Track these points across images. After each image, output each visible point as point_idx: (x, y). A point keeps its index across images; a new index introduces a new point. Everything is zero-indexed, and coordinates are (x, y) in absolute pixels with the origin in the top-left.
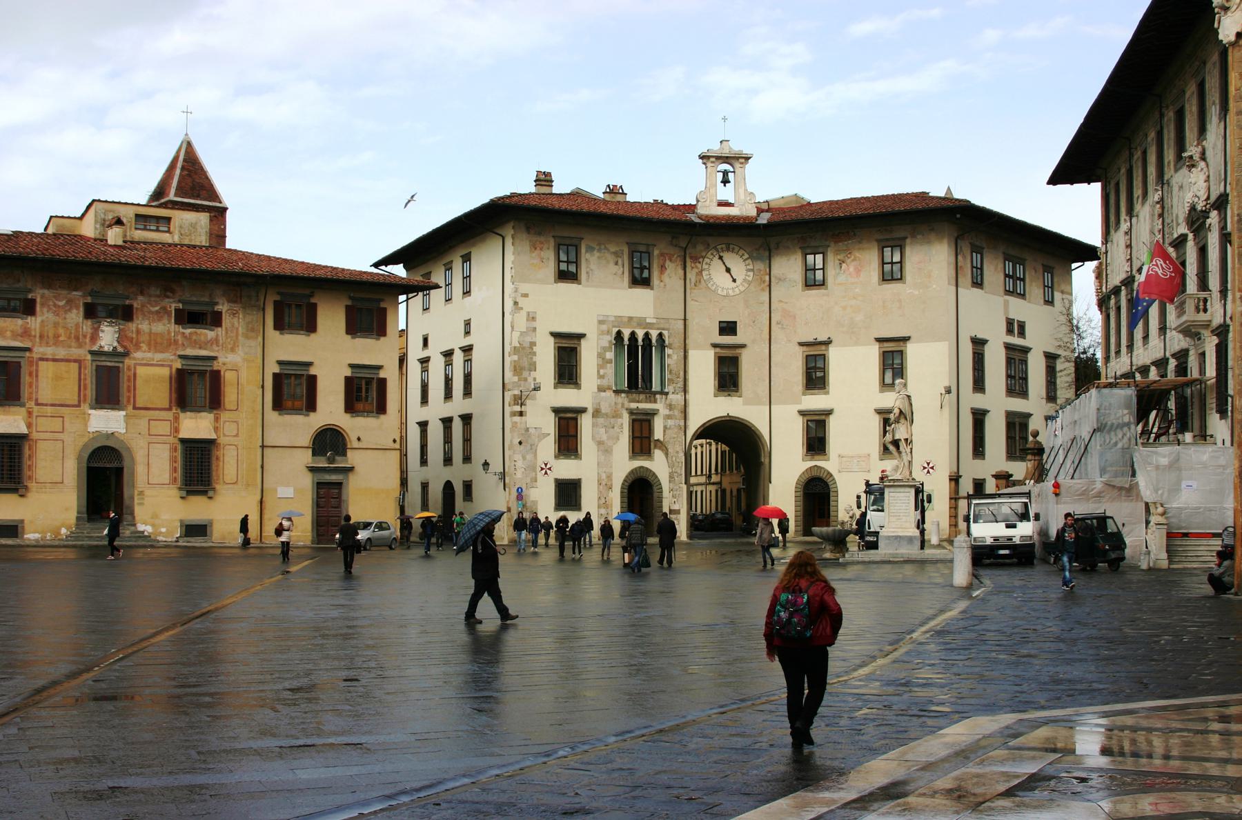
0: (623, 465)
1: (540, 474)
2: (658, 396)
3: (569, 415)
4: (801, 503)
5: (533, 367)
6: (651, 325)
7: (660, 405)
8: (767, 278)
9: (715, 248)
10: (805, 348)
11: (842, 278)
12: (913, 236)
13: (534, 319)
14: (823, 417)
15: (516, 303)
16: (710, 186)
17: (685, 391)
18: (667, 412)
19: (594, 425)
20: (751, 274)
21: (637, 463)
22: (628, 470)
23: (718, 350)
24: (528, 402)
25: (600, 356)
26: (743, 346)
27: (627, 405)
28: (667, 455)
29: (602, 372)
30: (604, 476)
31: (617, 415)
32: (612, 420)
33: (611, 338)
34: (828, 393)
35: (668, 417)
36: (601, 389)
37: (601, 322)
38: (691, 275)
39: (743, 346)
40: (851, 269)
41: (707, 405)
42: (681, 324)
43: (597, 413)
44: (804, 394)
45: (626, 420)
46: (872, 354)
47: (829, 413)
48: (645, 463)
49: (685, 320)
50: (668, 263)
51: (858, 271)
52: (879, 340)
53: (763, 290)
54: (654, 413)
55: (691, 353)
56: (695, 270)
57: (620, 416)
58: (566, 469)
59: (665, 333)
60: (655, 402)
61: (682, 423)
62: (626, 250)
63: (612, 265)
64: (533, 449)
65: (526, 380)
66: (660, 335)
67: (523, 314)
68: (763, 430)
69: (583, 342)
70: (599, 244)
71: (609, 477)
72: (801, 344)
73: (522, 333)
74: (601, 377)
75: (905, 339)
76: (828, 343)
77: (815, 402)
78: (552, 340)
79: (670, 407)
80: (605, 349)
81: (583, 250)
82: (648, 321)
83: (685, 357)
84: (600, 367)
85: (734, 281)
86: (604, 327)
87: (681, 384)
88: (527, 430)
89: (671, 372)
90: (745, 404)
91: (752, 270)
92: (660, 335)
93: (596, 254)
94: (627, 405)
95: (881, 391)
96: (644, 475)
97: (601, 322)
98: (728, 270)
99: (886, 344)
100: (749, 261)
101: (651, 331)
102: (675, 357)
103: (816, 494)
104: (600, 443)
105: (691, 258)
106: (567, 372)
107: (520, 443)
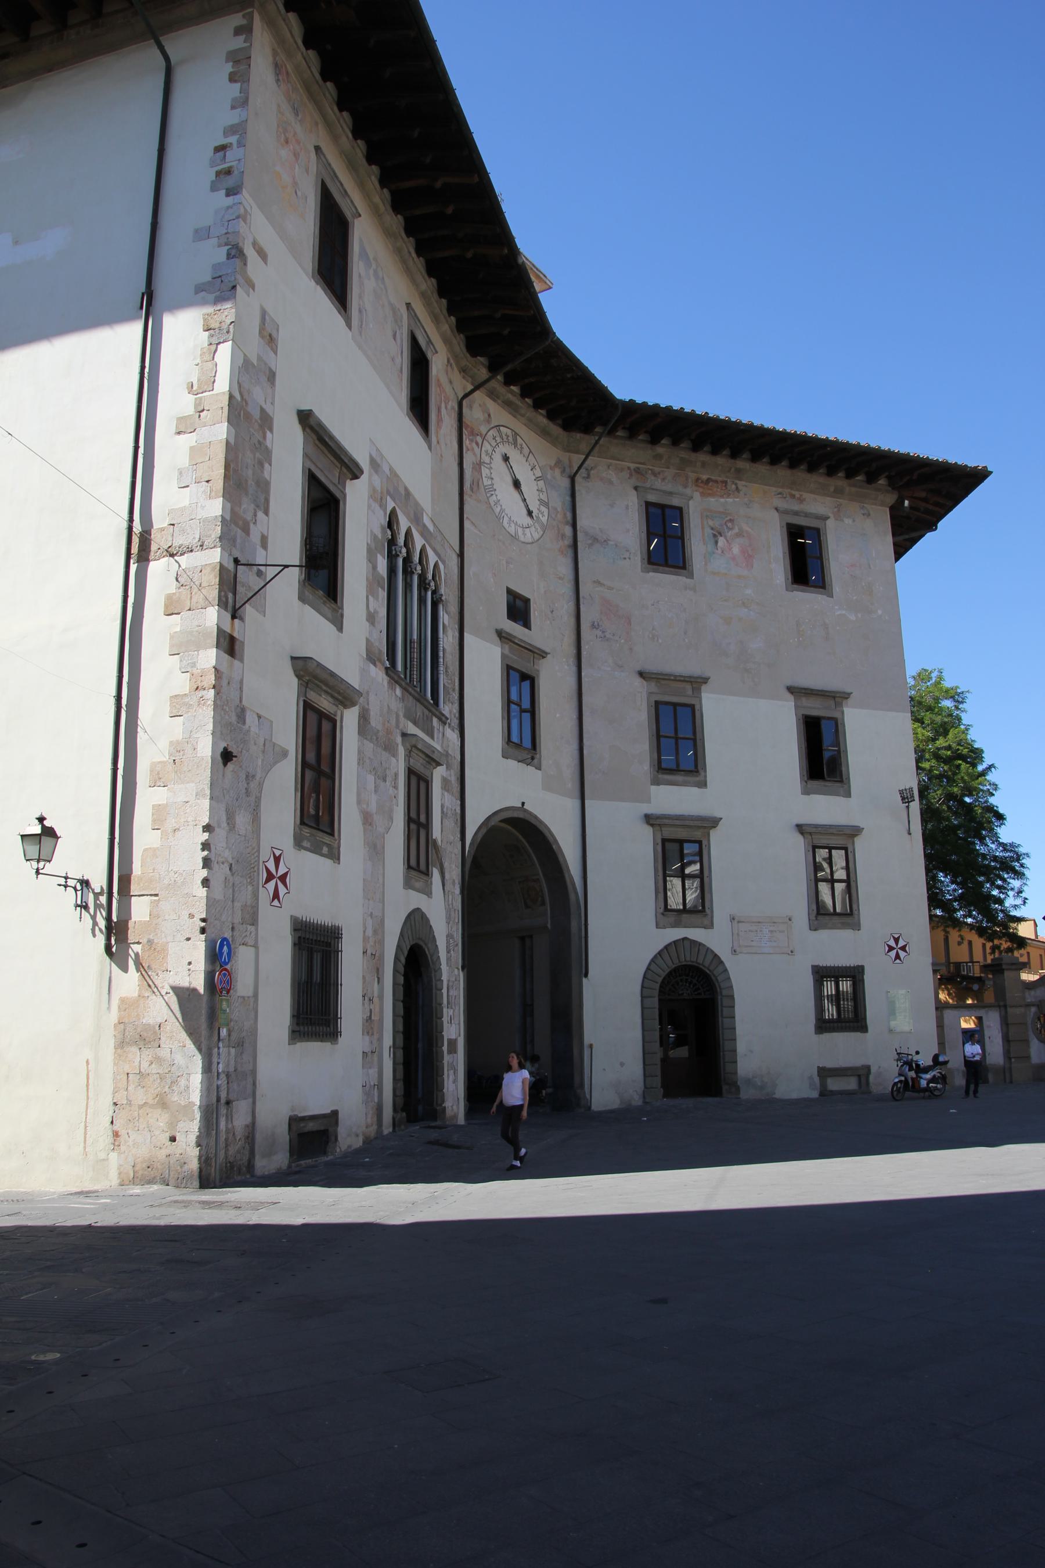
0: (400, 901)
3: (325, 703)
8: (568, 531)
10: (653, 687)
12: (838, 518)
13: (271, 340)
14: (697, 835)
15: (236, 253)
21: (416, 900)
26: (543, 654)
33: (381, 519)
34: (703, 784)
39: (543, 654)
44: (656, 782)
45: (399, 766)
47: (713, 822)
51: (748, 557)
61: (458, 811)
65: (246, 530)
71: (379, 929)
75: (846, 696)
76: (697, 683)
77: (676, 799)
82: (426, 521)
88: (241, 714)
90: (547, 786)
91: (546, 504)
94: (402, 719)
98: (517, 484)
99: (805, 702)
100: (541, 483)
103: (689, 1003)
104: (367, 819)
106: (322, 567)
107: (227, 756)
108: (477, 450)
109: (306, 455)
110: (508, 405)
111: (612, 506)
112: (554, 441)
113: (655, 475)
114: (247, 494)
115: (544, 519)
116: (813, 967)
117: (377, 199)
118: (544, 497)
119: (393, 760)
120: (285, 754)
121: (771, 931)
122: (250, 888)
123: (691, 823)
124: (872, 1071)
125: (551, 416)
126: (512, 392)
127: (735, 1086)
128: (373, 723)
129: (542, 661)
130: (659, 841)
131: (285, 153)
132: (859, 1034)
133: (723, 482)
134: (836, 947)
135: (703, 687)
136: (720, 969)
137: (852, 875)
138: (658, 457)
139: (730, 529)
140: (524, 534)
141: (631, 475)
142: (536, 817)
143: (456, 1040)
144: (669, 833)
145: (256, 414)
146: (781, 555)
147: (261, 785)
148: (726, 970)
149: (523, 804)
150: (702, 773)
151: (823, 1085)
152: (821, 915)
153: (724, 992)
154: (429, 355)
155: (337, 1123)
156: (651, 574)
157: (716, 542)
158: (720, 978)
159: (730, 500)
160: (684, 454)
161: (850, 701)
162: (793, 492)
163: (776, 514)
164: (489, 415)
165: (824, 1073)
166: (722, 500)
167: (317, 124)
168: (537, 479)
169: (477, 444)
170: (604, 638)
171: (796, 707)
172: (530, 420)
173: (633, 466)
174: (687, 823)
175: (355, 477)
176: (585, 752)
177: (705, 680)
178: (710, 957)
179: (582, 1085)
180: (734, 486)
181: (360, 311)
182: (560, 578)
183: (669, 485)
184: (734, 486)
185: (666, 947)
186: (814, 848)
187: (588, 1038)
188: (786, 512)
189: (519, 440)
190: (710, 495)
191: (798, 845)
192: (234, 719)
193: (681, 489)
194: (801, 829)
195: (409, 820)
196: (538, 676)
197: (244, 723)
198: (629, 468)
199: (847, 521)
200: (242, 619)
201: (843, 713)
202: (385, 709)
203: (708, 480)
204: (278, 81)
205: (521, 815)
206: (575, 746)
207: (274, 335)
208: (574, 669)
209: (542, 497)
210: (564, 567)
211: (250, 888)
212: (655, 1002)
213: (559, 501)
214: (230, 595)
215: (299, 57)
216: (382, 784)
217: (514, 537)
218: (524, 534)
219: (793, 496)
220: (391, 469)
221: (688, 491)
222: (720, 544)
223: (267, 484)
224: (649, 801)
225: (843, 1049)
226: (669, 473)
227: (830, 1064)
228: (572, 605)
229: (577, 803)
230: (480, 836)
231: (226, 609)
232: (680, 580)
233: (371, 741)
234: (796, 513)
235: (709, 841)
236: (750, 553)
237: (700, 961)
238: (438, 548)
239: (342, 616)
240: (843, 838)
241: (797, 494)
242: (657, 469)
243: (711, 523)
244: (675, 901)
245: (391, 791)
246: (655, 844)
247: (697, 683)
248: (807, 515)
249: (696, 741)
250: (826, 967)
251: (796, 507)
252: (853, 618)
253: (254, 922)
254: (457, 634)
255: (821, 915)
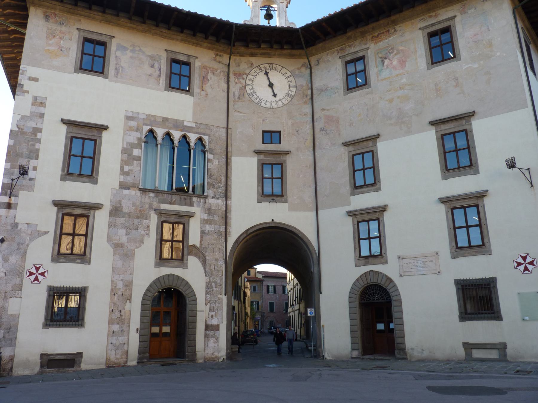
0: (146, 272)
1: (27, 282)
2: (195, 199)
4: (357, 316)
5: (35, 154)
6: (190, 129)
7: (197, 210)
8: (309, 92)
9: (259, 67)
10: (351, 148)
11: (385, 73)
12: (463, 12)
13: (42, 104)
14: (376, 216)
16: (255, 15)
17: (227, 196)
18: (206, 216)
19: (110, 225)
20: (294, 89)
21: (166, 271)
22: (153, 278)
23: (262, 157)
24: (22, 194)
25: (127, 151)
26: (288, 153)
27: (155, 205)
28: (204, 262)
29: (126, 168)
30: (120, 285)
31: (142, 215)
32: (136, 221)
34: (379, 189)
35: (205, 222)
36: (123, 186)
37: (129, 118)
38: (235, 89)
40: (395, 62)
41: (249, 212)
42: (223, 132)
43: (116, 211)
44: (353, 194)
46: (428, 141)
47: (382, 209)
48: (177, 271)
49: (227, 128)
50: (210, 75)
51: (402, 63)
52: (433, 123)
53: (306, 103)
54: (191, 215)
55: (236, 162)
56: (239, 85)
57: (148, 218)
58: (66, 275)
59: (206, 138)
60: (191, 204)
61: (223, 229)
62: (164, 57)
63: (146, 67)
64: (22, 251)
66: (200, 139)
67: (28, 98)
68: (311, 237)
69: (105, 134)
70: (134, 46)
71: (128, 285)
72: (346, 144)
73: (23, 118)
74: (123, 173)
75: (471, 115)
76: (375, 138)
78: (64, 128)
79: (209, 211)
80: (132, 146)
81: (113, 46)
82: (186, 124)
83: (227, 164)
84: (124, 163)
85: (275, 95)
86: (133, 124)
87: (222, 189)
88: (16, 225)
89: (211, 177)
90: (291, 209)
91: (295, 86)
92: (200, 139)
93: (129, 54)
95: (445, 178)
96: (174, 285)
97: (129, 118)
98: (271, 85)
99: (443, 127)
100: (292, 78)
101: (188, 134)
102: (216, 162)
103: (376, 305)
104: (117, 246)
105: (235, 74)
108: (243, 81)
109: (68, 132)
110: (263, 55)
111: (329, 72)
112: (300, 56)
113: (350, 46)
114: (22, 157)
115: (293, 93)
116: (455, 280)
117: (129, 25)
118: (293, 83)
119: (145, 222)
120: (47, 233)
121: (424, 262)
122: (18, 279)
123: (370, 211)
124: (508, 346)
125: (293, 48)
126: (264, 49)
127: (403, 350)
128: (125, 209)
129: (288, 156)
130: (356, 223)
131: (51, 42)
132: (495, 322)
133: (386, 32)
134: (474, 268)
135: (378, 140)
136: (391, 285)
137: (482, 221)
138: (349, 38)
139: (392, 53)
140: (277, 104)
141: (338, 53)
142: (284, 224)
143: (218, 325)
144: (360, 218)
145: (31, 130)
146: (424, 52)
147: (28, 245)
148: (395, 285)
149: (273, 220)
150: (378, 183)
151: (468, 354)
152: (458, 250)
153: (394, 298)
154: (192, 60)
155: (81, 357)
156: (349, 95)
157: (383, 64)
158: (391, 291)
159: (391, 38)
160: (361, 29)
161: (476, 116)
162: (431, 14)
163: (420, 31)
164: (252, 64)
165: (468, 347)
166: (387, 40)
167: (80, 20)
168: (287, 78)
169: (243, 79)
170: (327, 134)
171: (437, 132)
172: (280, 55)
173: (339, 48)
174: (367, 211)
175: (106, 129)
176: (318, 189)
177: (378, 136)
178: (385, 279)
179: (320, 346)
180: (393, 30)
181: (116, 69)
182: (304, 115)
183: (355, 48)
184: (393, 30)
185: (360, 277)
186: (452, 209)
187: (322, 323)
188: (426, 27)
189: (274, 66)
190: (380, 41)
191: (442, 208)
192: (9, 228)
193: (364, 47)
194: (444, 201)
195: (161, 241)
196: (285, 162)
197: (17, 228)
198: (337, 50)
199: (470, 11)
200: (17, 196)
201: (471, 124)
202: (138, 203)
203: (378, 35)
204: (47, 20)
205: (273, 225)
206: (314, 187)
207: (44, 101)
208: (313, 152)
209: (291, 83)
210: (307, 109)
211: (18, 279)
212: (357, 304)
213: (303, 82)
214: (9, 192)
215: (58, 7)
216: (134, 232)
217: (271, 108)
218: (277, 104)
219: (431, 16)
220: (147, 115)
221: (367, 46)
222: (385, 64)
223: (38, 151)
224: (349, 204)
225: (481, 331)
226: (357, 43)
227: (471, 341)
228: (312, 124)
229: (315, 212)
230: (242, 238)
231: (6, 195)
232: (365, 90)
233: (123, 217)
234: (433, 25)
235: (383, 218)
236: (404, 59)
237: (379, 282)
238: (202, 131)
239: (97, 179)
240: (475, 201)
241: (434, 14)
242: (351, 44)
243: (380, 55)
244: (365, 252)
245: (143, 232)
246: (354, 225)
247: (375, 138)
248: (439, 22)
249: (375, 168)
250: (463, 280)
251: (433, 22)
252: (476, 66)
253: (21, 290)
254: (224, 160)
255: (458, 250)
